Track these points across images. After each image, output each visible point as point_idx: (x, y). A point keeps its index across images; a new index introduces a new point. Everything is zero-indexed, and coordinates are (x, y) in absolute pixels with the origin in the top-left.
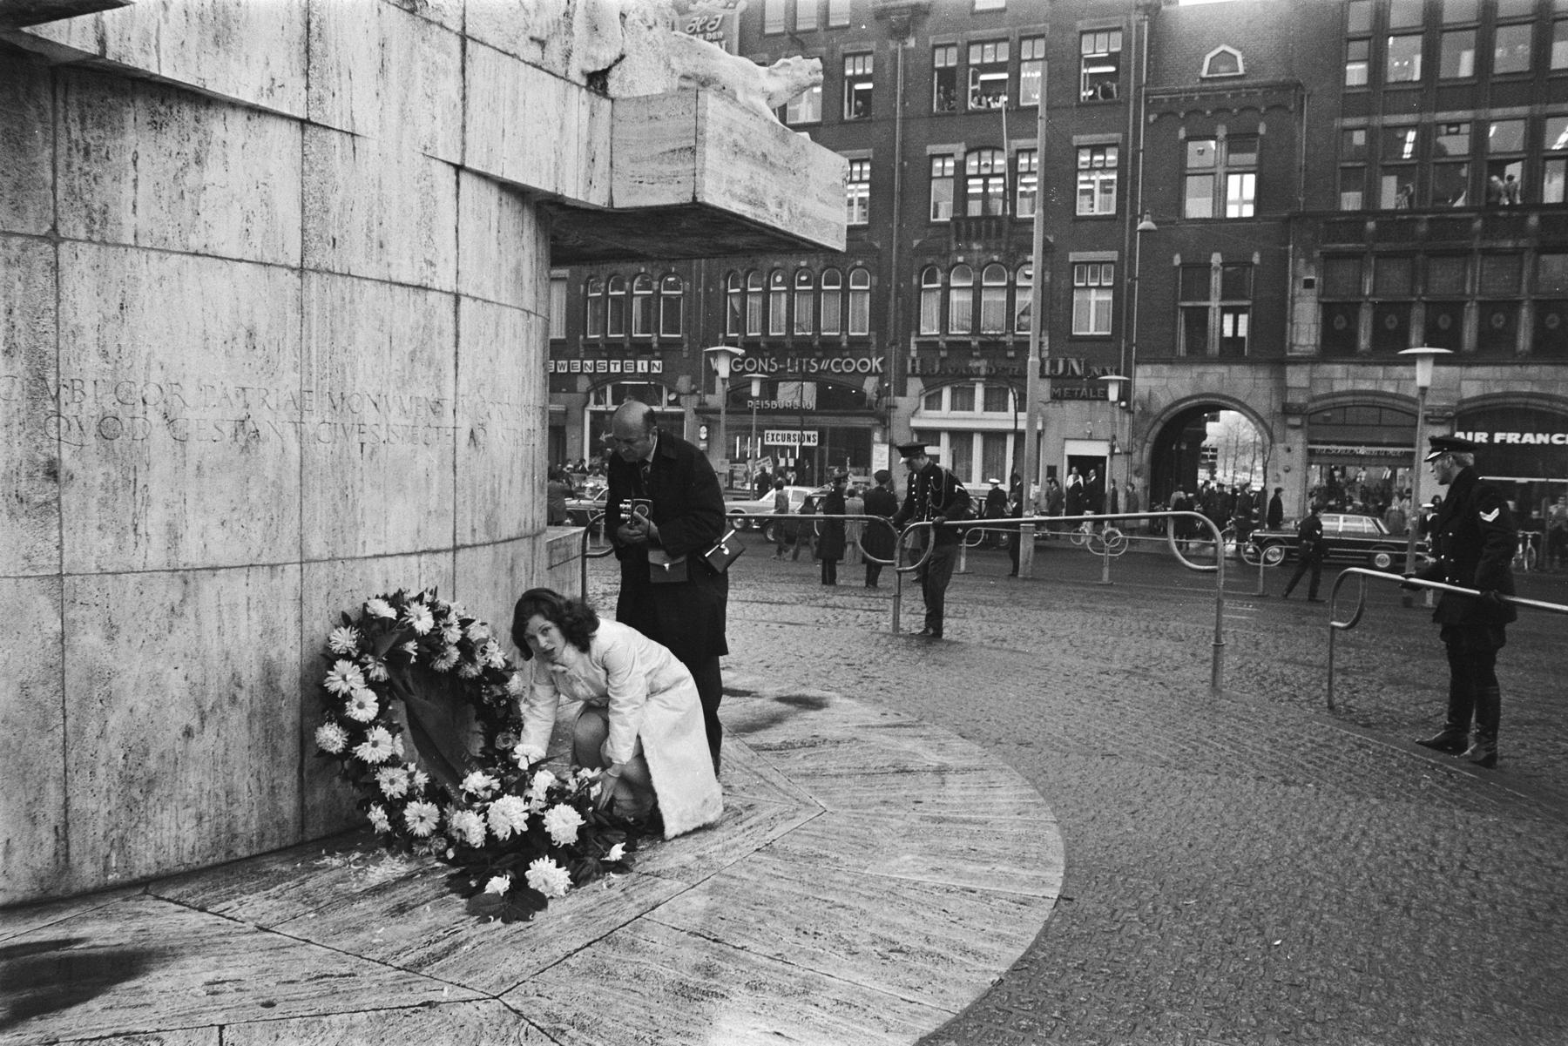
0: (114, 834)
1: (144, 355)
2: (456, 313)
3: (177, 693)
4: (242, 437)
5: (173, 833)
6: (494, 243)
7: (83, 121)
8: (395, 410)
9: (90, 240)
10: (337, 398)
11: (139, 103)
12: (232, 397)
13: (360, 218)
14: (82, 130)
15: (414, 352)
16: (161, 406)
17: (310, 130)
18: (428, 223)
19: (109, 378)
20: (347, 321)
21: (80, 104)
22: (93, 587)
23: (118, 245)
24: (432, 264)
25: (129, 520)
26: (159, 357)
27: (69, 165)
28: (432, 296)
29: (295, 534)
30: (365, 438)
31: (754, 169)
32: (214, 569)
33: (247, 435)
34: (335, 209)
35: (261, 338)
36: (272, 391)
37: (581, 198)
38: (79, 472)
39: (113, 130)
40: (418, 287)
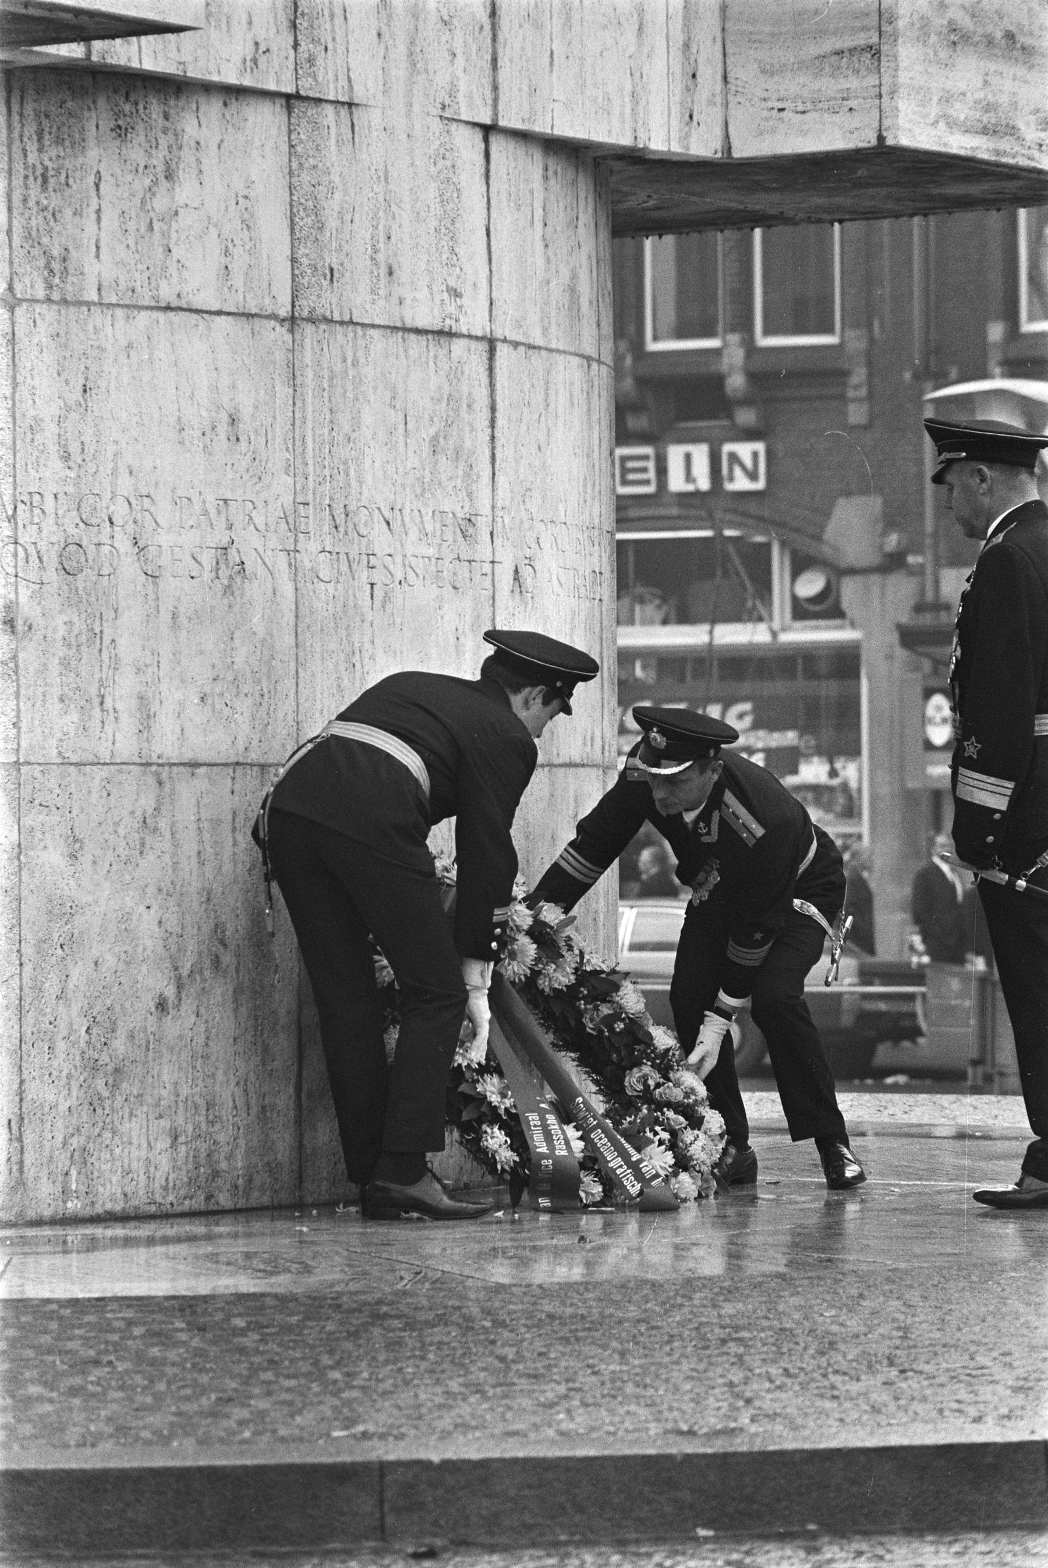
0: (74, 1142)
1: (110, 456)
2: (491, 369)
3: (148, 943)
4: (224, 573)
5: (143, 1154)
6: (539, 246)
7: (40, 139)
8: (414, 534)
9: (49, 300)
10: (339, 512)
11: (102, 102)
12: (213, 514)
13: (363, 233)
14: (40, 150)
15: (435, 438)
16: (130, 528)
17: (299, 107)
18: (449, 227)
19: (71, 489)
20: (350, 395)
21: (37, 115)
22: (53, 783)
23: (79, 303)
24: (456, 294)
25: (93, 690)
26: (129, 459)
27: (25, 200)
28: (459, 346)
29: (290, 718)
30: (378, 576)
31: (992, 66)
32: (194, 765)
33: (230, 570)
34: (332, 224)
35: (246, 426)
36: (260, 505)
37: (676, 148)
38: (39, 621)
39: (73, 144)
40: (440, 333)
